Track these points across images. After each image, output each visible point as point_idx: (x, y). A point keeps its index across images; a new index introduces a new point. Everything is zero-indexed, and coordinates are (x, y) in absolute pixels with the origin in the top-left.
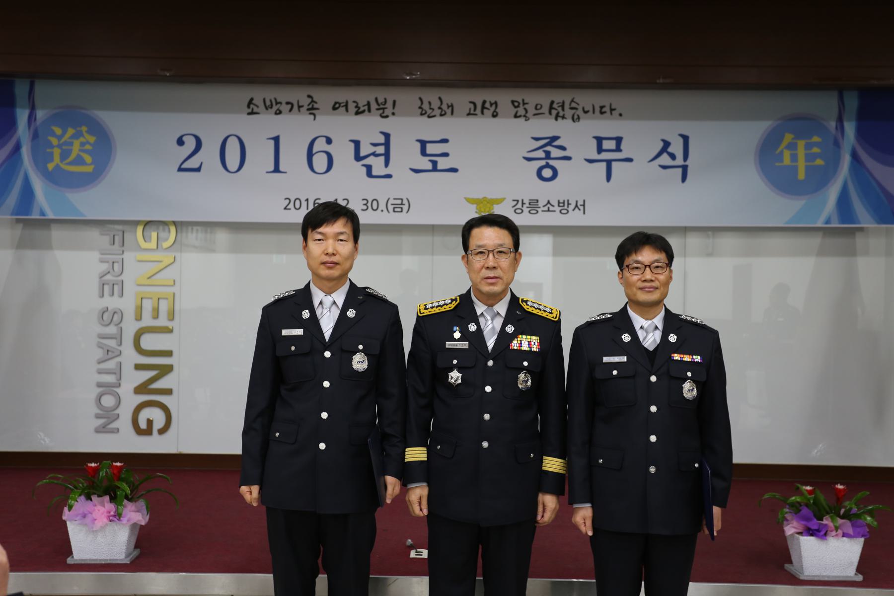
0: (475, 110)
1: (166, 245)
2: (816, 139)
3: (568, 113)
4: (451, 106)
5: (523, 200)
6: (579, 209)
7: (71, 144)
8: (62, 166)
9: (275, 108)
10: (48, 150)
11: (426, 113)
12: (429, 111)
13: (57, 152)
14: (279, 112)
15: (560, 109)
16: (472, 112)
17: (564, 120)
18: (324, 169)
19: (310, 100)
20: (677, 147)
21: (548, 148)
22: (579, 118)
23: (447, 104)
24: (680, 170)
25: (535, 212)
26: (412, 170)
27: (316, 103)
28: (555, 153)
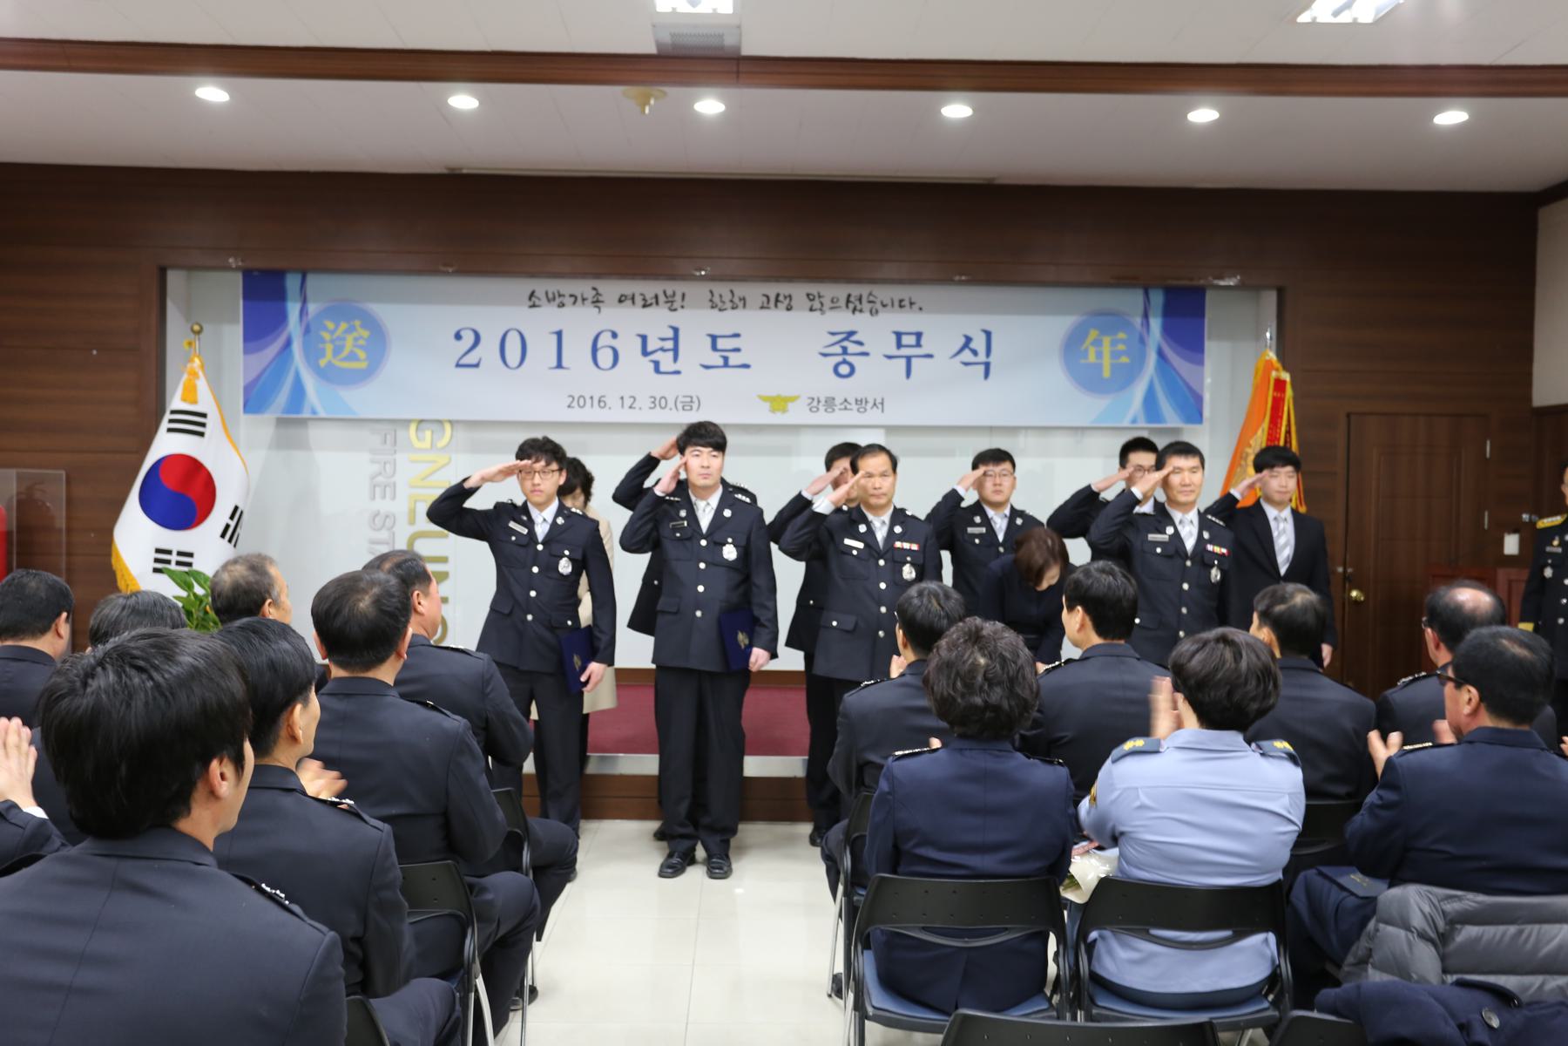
2: (1122, 335)
3: (866, 306)
4: (743, 299)
6: (877, 408)
7: (344, 339)
8: (337, 363)
12: (720, 304)
13: (329, 348)
14: (562, 305)
15: (857, 303)
16: (765, 305)
19: (594, 292)
20: (979, 343)
21: (845, 344)
22: (877, 312)
24: (982, 368)
27: (600, 295)
28: (852, 348)
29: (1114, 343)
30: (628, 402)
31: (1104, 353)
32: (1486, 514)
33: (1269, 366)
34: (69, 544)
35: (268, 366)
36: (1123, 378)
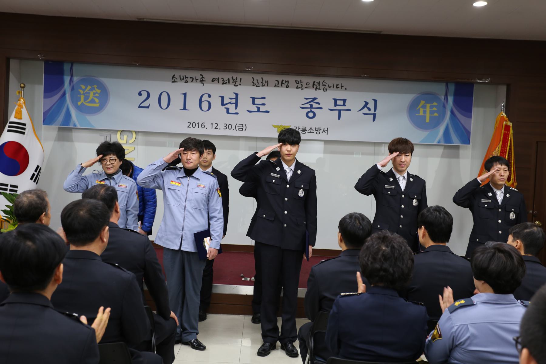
0: (278, 84)
2: (435, 104)
3: (322, 87)
5: (299, 127)
6: (325, 132)
7: (90, 93)
10: (78, 96)
12: (257, 84)
14: (187, 82)
15: (318, 85)
16: (277, 85)
17: (320, 90)
18: (207, 109)
19: (201, 77)
20: (371, 105)
21: (312, 103)
22: (326, 90)
23: (266, 81)
24: (372, 115)
25: (305, 133)
27: (204, 78)
28: (315, 105)
29: (431, 107)
30: (214, 126)
33: (502, 119)
36: (435, 123)
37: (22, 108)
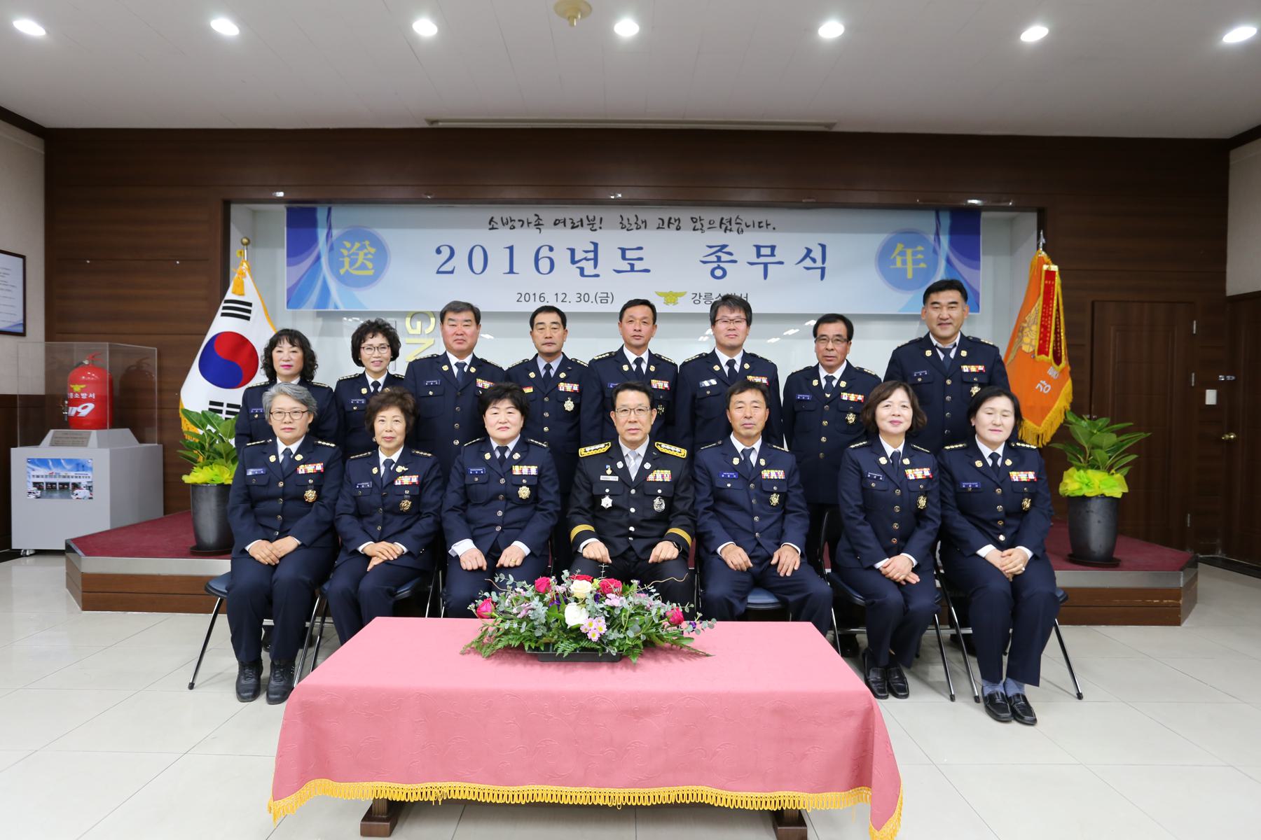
0: (663, 225)
1: (427, 331)
2: (920, 248)
3: (735, 227)
4: (645, 222)
7: (358, 254)
9: (510, 224)
10: (341, 259)
11: (625, 227)
12: (628, 226)
13: (347, 260)
14: (513, 228)
15: (728, 224)
19: (536, 218)
20: (817, 254)
21: (719, 254)
22: (742, 231)
24: (820, 270)
26: (615, 271)
28: (725, 257)
31: (908, 261)
32: (1193, 375)
34: (160, 401)
35: (304, 274)
37: (245, 277)
